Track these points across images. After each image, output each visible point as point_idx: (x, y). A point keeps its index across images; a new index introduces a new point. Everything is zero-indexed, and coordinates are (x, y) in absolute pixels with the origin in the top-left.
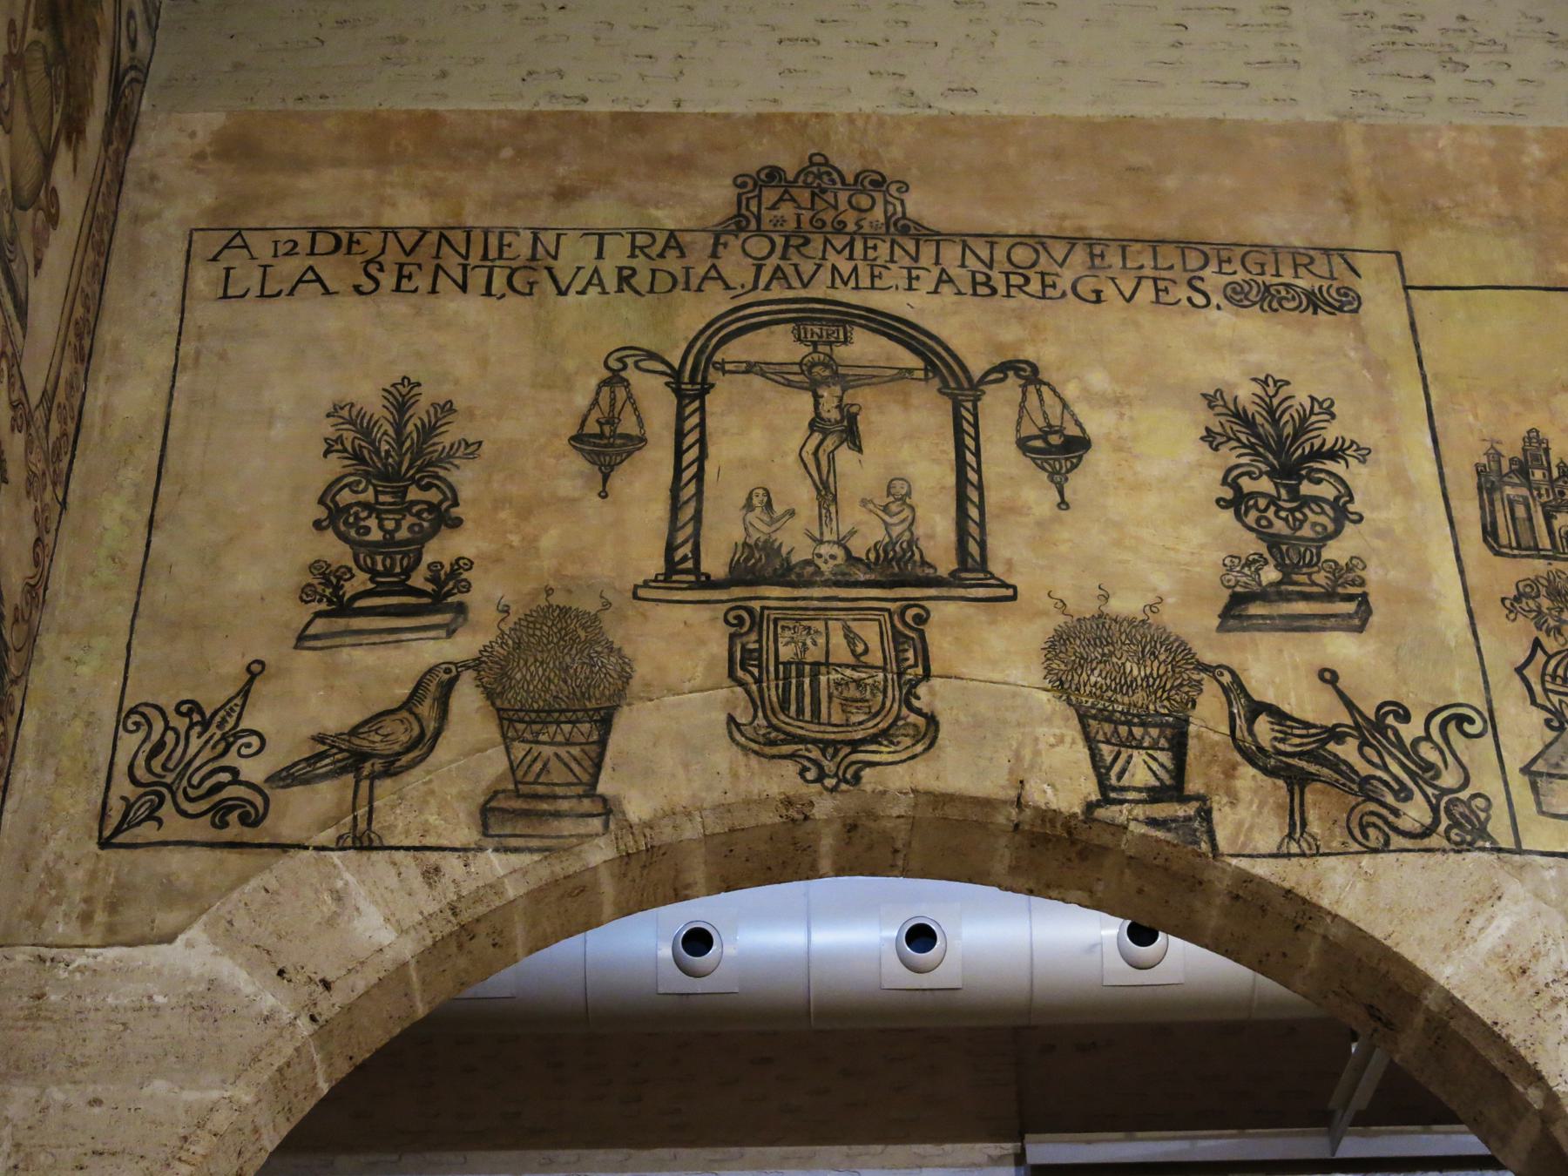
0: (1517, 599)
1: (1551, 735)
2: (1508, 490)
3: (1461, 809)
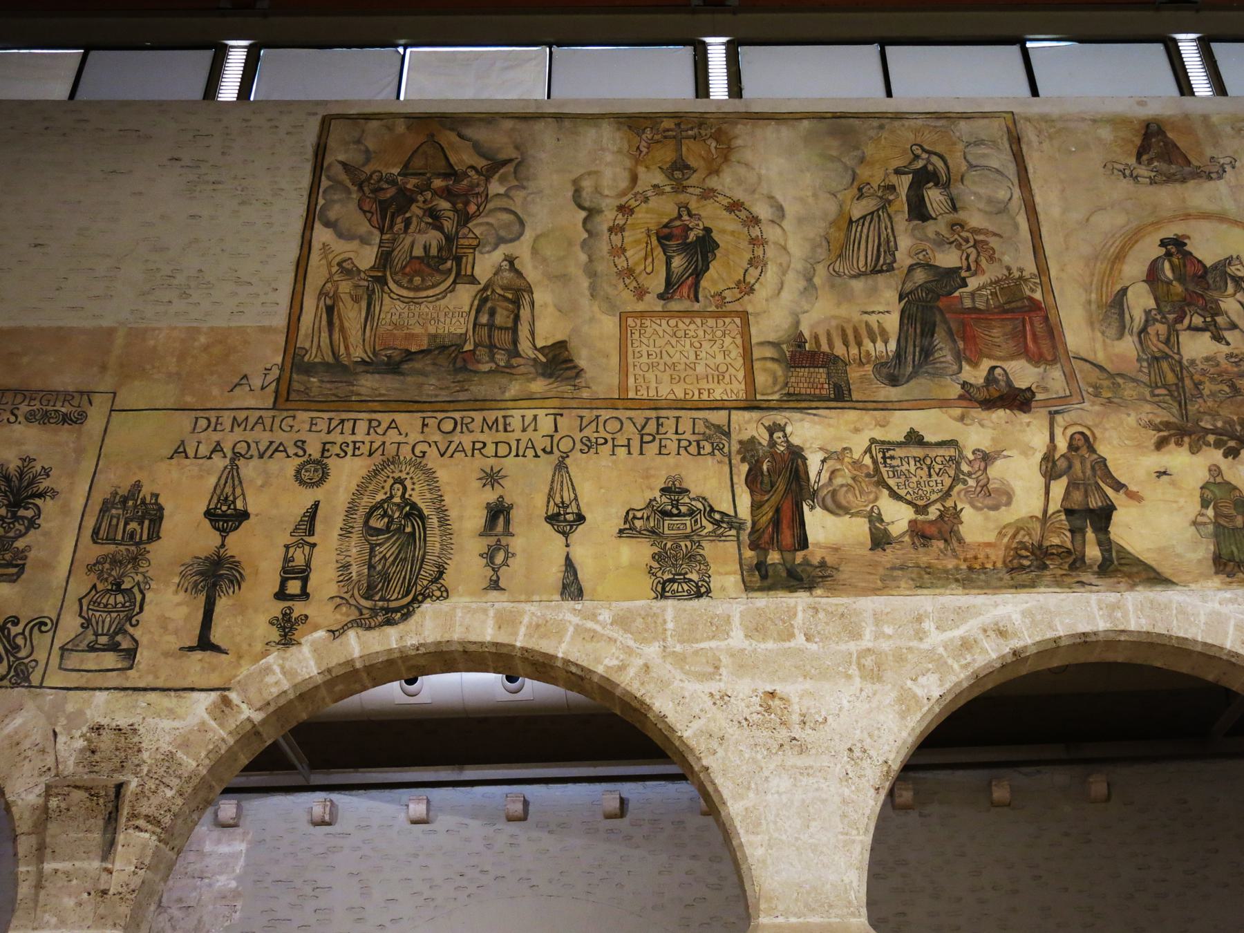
0: (95, 565)
1: (81, 630)
2: (114, 511)
3: (23, 667)
